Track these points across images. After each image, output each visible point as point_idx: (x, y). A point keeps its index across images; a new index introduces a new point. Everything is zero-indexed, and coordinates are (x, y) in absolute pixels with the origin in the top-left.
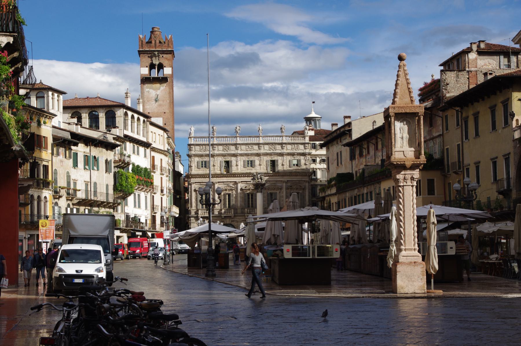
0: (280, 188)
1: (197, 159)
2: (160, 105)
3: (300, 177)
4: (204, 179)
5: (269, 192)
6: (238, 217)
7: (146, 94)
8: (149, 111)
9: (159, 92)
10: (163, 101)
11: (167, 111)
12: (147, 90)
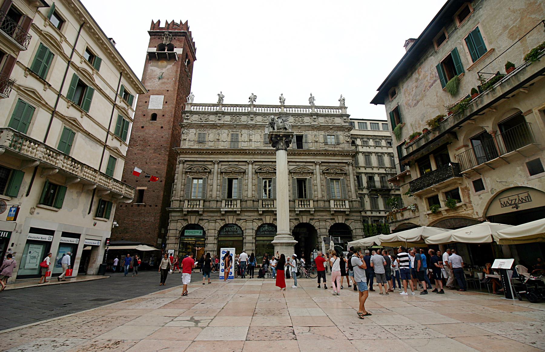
0: (311, 171)
1: (193, 131)
3: (340, 158)
4: (200, 156)
6: (246, 214)
7: (149, 71)
8: (149, 89)
9: (164, 70)
10: (168, 79)
12: (151, 68)
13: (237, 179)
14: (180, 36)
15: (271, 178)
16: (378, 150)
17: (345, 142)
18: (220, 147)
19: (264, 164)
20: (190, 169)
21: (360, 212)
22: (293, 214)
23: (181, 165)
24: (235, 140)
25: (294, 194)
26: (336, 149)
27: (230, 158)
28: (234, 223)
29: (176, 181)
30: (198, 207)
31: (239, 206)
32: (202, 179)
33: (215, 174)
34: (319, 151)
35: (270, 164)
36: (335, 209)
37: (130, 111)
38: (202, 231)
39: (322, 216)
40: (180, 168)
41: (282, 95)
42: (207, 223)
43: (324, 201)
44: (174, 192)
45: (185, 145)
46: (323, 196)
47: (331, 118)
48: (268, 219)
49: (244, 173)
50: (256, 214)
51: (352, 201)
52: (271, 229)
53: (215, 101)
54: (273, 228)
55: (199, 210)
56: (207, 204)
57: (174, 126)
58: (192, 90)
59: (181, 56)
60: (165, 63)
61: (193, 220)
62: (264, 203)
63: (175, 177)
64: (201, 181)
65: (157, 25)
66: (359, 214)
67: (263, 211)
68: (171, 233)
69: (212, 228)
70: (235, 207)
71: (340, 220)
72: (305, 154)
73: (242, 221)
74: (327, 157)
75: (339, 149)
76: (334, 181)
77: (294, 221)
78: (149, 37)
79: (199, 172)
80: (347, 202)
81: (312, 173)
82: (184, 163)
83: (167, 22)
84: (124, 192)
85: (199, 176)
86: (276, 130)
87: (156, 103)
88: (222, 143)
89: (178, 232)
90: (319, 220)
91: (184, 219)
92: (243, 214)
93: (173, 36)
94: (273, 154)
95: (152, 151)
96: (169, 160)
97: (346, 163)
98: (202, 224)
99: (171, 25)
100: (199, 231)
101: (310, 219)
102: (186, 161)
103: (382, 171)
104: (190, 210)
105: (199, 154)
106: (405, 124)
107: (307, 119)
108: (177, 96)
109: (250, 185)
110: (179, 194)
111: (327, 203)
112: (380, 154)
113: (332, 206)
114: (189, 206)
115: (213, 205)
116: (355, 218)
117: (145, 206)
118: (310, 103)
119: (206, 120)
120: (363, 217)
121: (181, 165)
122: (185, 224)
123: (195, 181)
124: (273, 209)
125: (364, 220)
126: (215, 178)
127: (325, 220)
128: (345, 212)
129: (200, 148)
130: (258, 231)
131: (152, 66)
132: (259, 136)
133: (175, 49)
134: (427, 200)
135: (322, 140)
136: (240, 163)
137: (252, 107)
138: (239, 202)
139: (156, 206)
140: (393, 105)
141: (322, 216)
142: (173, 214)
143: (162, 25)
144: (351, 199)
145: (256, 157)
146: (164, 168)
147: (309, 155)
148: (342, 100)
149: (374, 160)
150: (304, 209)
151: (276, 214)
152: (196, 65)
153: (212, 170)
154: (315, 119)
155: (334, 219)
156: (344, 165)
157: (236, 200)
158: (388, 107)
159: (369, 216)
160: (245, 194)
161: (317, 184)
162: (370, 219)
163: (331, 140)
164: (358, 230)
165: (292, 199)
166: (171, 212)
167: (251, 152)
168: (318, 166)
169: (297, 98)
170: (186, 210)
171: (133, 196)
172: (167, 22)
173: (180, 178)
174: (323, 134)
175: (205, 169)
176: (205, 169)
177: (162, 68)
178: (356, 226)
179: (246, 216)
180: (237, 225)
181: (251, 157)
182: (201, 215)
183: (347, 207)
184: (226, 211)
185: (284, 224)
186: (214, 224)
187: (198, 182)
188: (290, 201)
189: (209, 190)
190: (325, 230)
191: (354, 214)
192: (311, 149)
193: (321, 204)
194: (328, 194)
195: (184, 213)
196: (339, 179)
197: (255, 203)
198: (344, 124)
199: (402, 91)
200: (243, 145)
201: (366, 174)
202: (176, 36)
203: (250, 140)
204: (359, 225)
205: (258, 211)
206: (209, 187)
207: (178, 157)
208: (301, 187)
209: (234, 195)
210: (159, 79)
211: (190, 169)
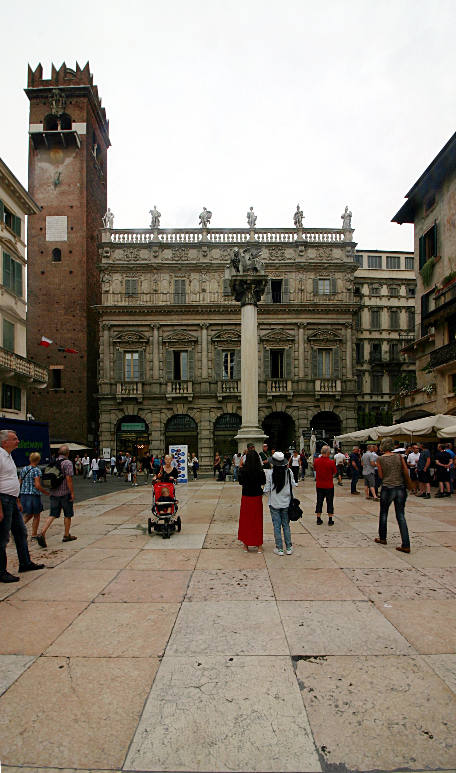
2: (62, 193)
4: (132, 318)
5: (268, 348)
6: (201, 401)
7: (37, 172)
9: (61, 168)
10: (69, 186)
11: (75, 203)
13: (186, 351)
14: (79, 96)
15: (234, 350)
16: (394, 302)
17: (345, 290)
18: (160, 303)
19: (224, 328)
20: (120, 338)
21: (356, 396)
22: (264, 400)
23: (106, 332)
24: (180, 291)
25: (265, 372)
26: (330, 302)
27: (175, 320)
28: (185, 413)
29: (101, 356)
30: (135, 392)
31: (190, 390)
32: (137, 352)
33: (156, 345)
34: (305, 305)
35: (233, 327)
36: (321, 393)
37: (19, 246)
38: (143, 425)
39: (303, 402)
40: (105, 337)
41: (251, 209)
42: (149, 414)
43: (307, 382)
44: (101, 372)
45: (109, 301)
46: (306, 375)
47: (327, 250)
48: (230, 408)
49: (196, 342)
50: (214, 401)
51: (345, 381)
52: (234, 420)
53: (147, 225)
54: (236, 420)
55: (138, 396)
56: (147, 388)
57: (88, 270)
58: (110, 205)
59: (85, 139)
60: (60, 154)
61: (131, 410)
62: (224, 386)
63: (101, 351)
64: (136, 356)
65: (38, 75)
66: (353, 399)
67: (223, 397)
68: (104, 427)
69: (156, 420)
70: (185, 391)
71: (327, 407)
72: (284, 312)
73: (195, 411)
74: (316, 316)
75: (334, 302)
76: (324, 353)
77: (265, 409)
78: (28, 102)
79: (133, 342)
80: (339, 383)
81: (293, 341)
82: (109, 329)
83: (53, 68)
84: (33, 373)
85: (134, 348)
86: (241, 273)
87: (57, 230)
88: (162, 297)
89: (113, 426)
90: (298, 408)
91: (118, 409)
92: (196, 401)
93: (67, 97)
94: (237, 311)
95: (62, 312)
96: (88, 326)
97: (343, 324)
98: (142, 415)
99: (62, 74)
100: (140, 424)
101: (287, 407)
102: (113, 326)
103: (395, 336)
104: (125, 396)
105: (130, 315)
106: (440, 257)
107: (289, 253)
108: (87, 216)
109: (205, 360)
110: (108, 375)
111: (311, 385)
112: (394, 310)
113: (318, 388)
114: (124, 391)
115: (156, 389)
116: (348, 404)
117: (65, 392)
118: (295, 223)
119: (136, 258)
120: (359, 402)
121: (106, 332)
122: (121, 416)
123: (128, 356)
124: (237, 394)
125: (360, 407)
126: (156, 351)
127: (307, 408)
128: (334, 396)
129: (130, 304)
130: (217, 424)
131: (40, 161)
132: (216, 284)
133: (74, 124)
134: (451, 378)
135: (309, 287)
136: (190, 328)
137: (205, 233)
138: (190, 384)
139: (80, 392)
140: (427, 225)
141: (303, 402)
142: (103, 403)
143: (47, 75)
144: (344, 378)
145: (212, 317)
146: (82, 337)
147: (289, 312)
148: (347, 217)
149: (385, 317)
150: (279, 394)
151: (240, 401)
152: (112, 154)
153: (151, 339)
154: (301, 251)
155: (318, 406)
156: (340, 327)
157: (186, 382)
158: (419, 227)
159: (367, 402)
160: (198, 373)
161: (299, 354)
162: (367, 405)
163: (325, 287)
164: (350, 421)
165: (262, 379)
166: (101, 399)
167: (204, 310)
168: (301, 330)
169: (275, 217)
170: (120, 396)
171: (46, 378)
172: (53, 68)
173: (107, 351)
174: (313, 277)
175: (141, 338)
176: (141, 338)
177: (56, 163)
178: (347, 415)
179: (201, 403)
180: (189, 416)
181: (205, 317)
182: (141, 403)
183: (339, 389)
184: (173, 398)
185: (251, 414)
186: (158, 415)
187: (132, 356)
188: (259, 382)
189: (148, 369)
190: (305, 422)
191: (346, 399)
192: (293, 302)
193: (303, 386)
194: (314, 371)
195: (118, 401)
196: (331, 349)
197: (212, 386)
198: (346, 260)
199: (446, 197)
200: (193, 299)
201: (370, 340)
202: (72, 96)
203: (204, 291)
204: (352, 414)
205: (216, 397)
206: (148, 363)
207: (101, 319)
208: (275, 363)
209: (184, 375)
210: (56, 185)
211: (120, 338)
